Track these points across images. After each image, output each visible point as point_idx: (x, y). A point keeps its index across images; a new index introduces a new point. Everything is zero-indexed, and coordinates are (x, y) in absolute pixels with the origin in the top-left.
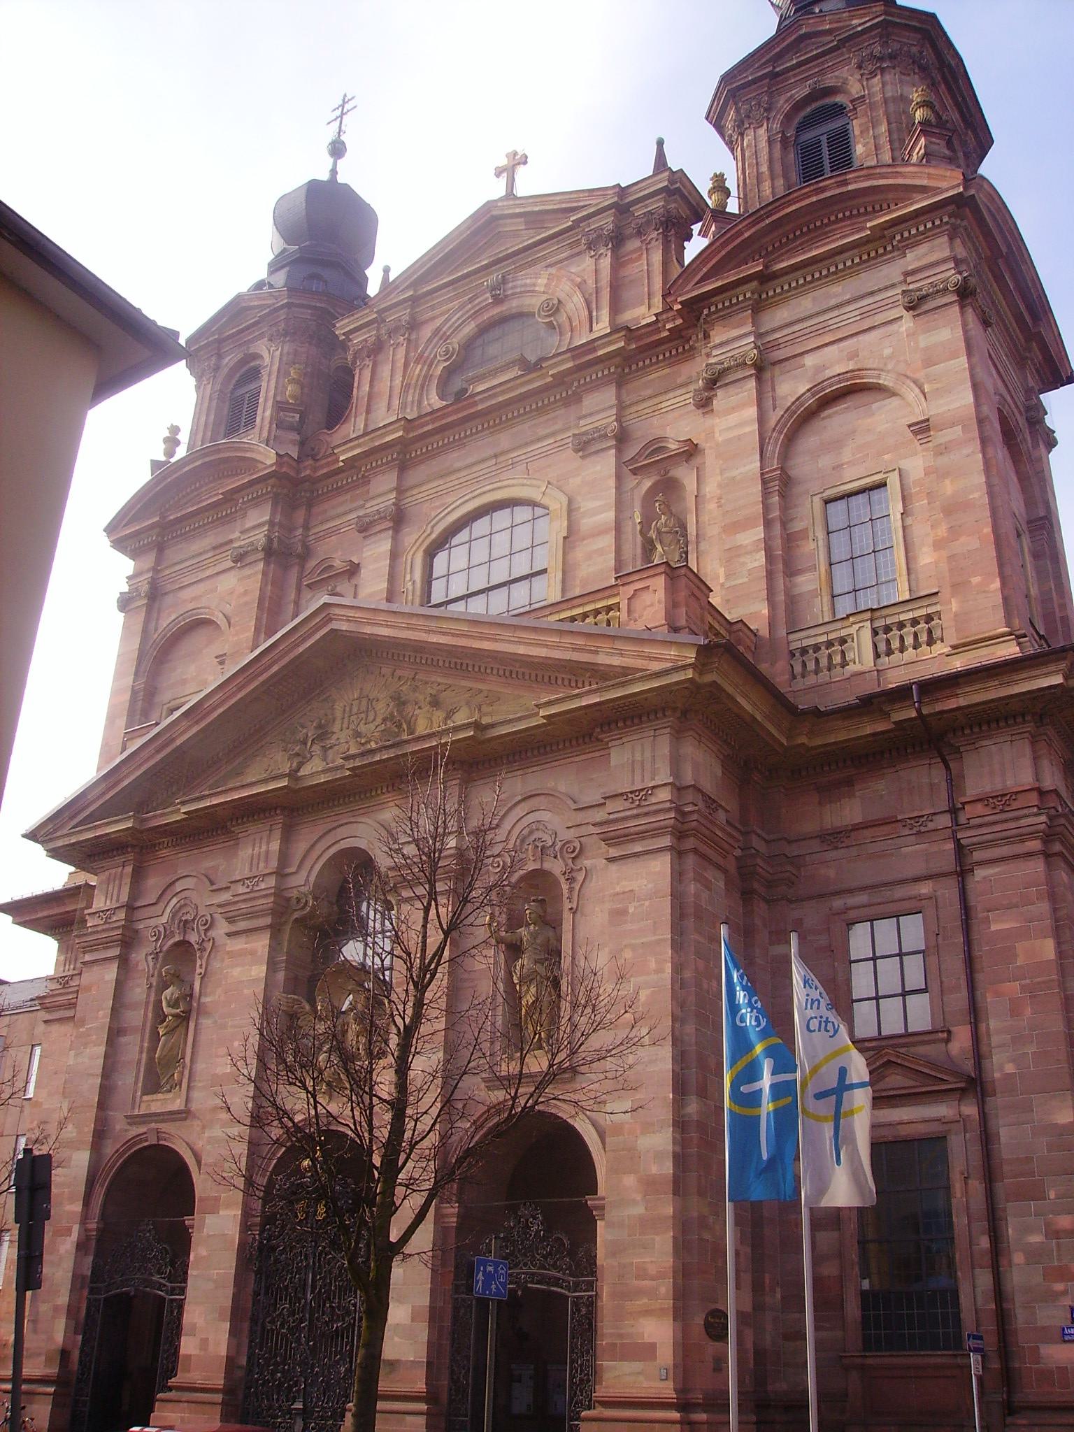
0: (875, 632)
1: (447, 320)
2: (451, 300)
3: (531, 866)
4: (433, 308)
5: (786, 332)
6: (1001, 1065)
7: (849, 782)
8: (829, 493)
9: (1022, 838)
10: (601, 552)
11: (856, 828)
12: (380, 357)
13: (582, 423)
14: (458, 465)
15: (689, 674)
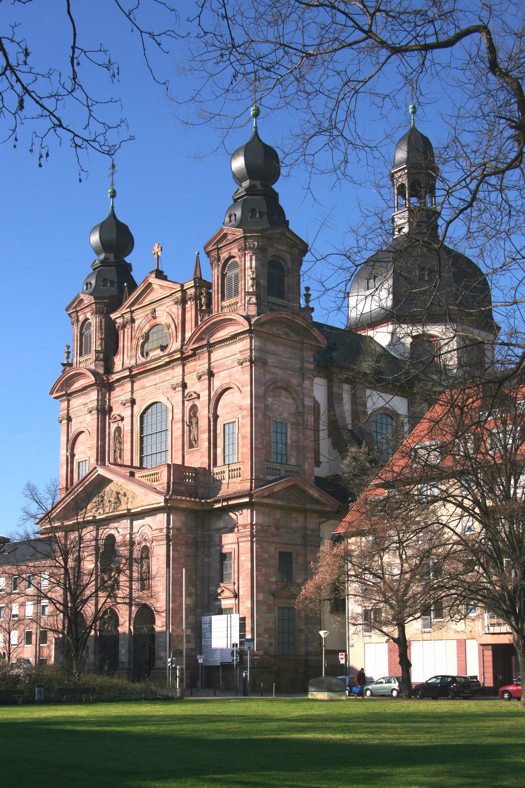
0: (229, 471)
1: (141, 322)
2: (142, 313)
3: (144, 544)
4: (137, 315)
5: (218, 362)
6: (241, 593)
7: (221, 515)
8: (225, 422)
9: (246, 536)
10: (178, 428)
11: (222, 528)
12: (126, 330)
13: (175, 379)
14: (147, 385)
15: (163, 504)
